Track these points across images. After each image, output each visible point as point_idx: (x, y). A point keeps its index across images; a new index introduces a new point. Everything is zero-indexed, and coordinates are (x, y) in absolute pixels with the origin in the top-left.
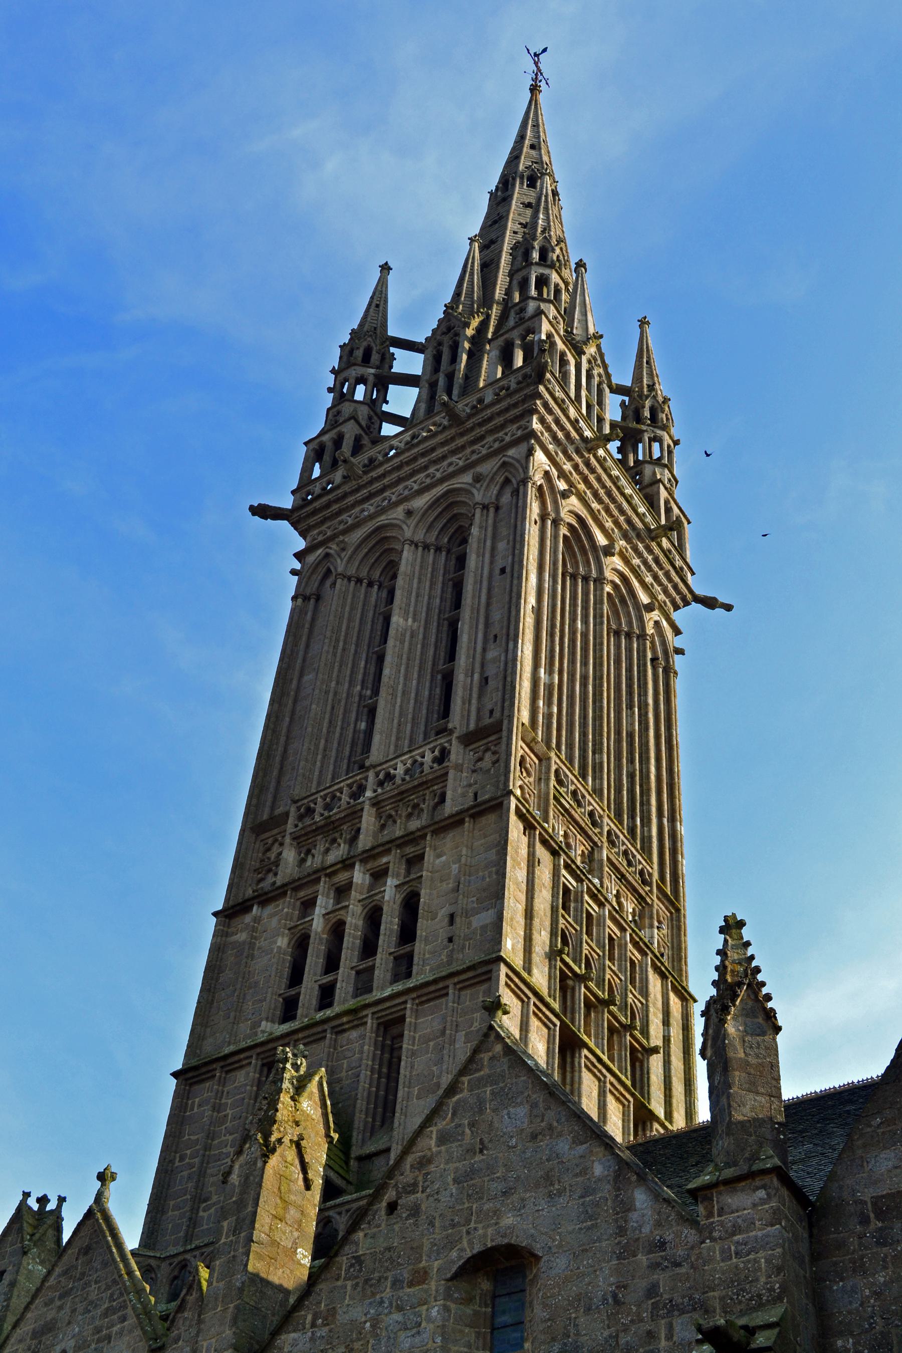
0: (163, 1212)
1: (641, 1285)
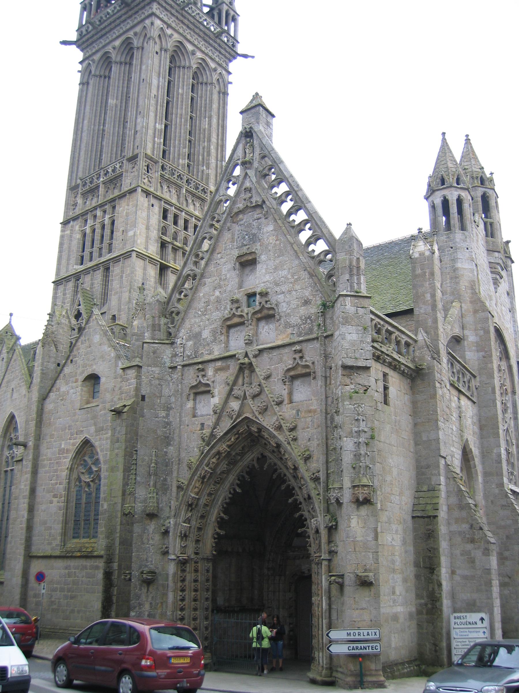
1: (118, 386)
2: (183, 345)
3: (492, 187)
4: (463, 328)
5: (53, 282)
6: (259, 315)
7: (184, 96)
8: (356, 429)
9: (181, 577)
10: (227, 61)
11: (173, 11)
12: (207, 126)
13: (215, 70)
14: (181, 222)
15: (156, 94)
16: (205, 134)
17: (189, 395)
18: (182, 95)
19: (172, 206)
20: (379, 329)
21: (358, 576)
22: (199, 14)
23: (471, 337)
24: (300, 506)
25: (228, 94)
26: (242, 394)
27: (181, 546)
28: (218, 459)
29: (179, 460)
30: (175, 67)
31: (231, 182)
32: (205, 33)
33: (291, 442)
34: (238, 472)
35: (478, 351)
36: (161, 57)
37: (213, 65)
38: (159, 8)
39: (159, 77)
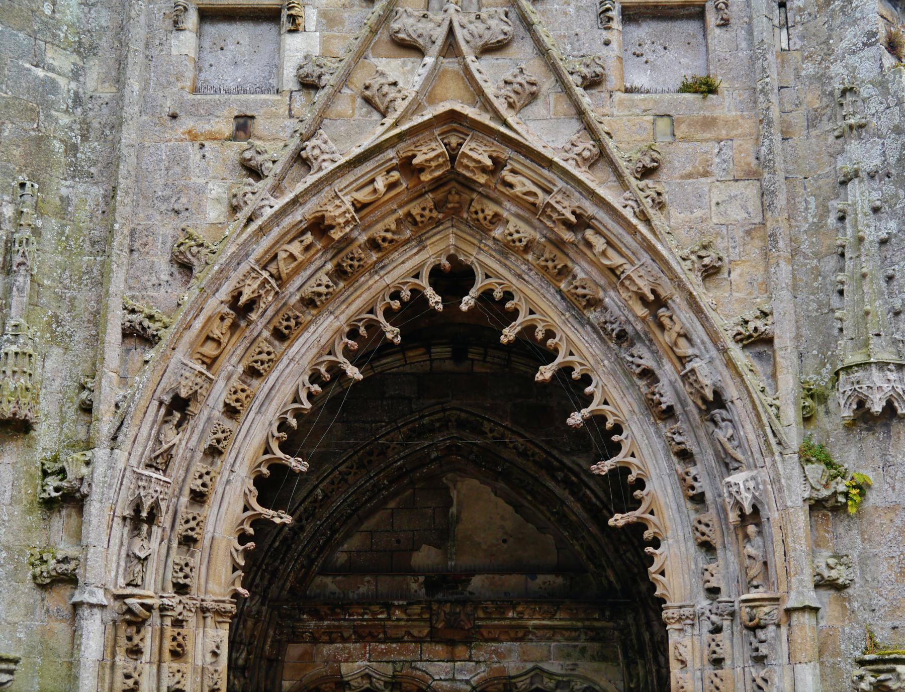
24: (615, 438)
26: (444, 29)
28: (307, 248)
33: (651, 212)
34: (354, 307)
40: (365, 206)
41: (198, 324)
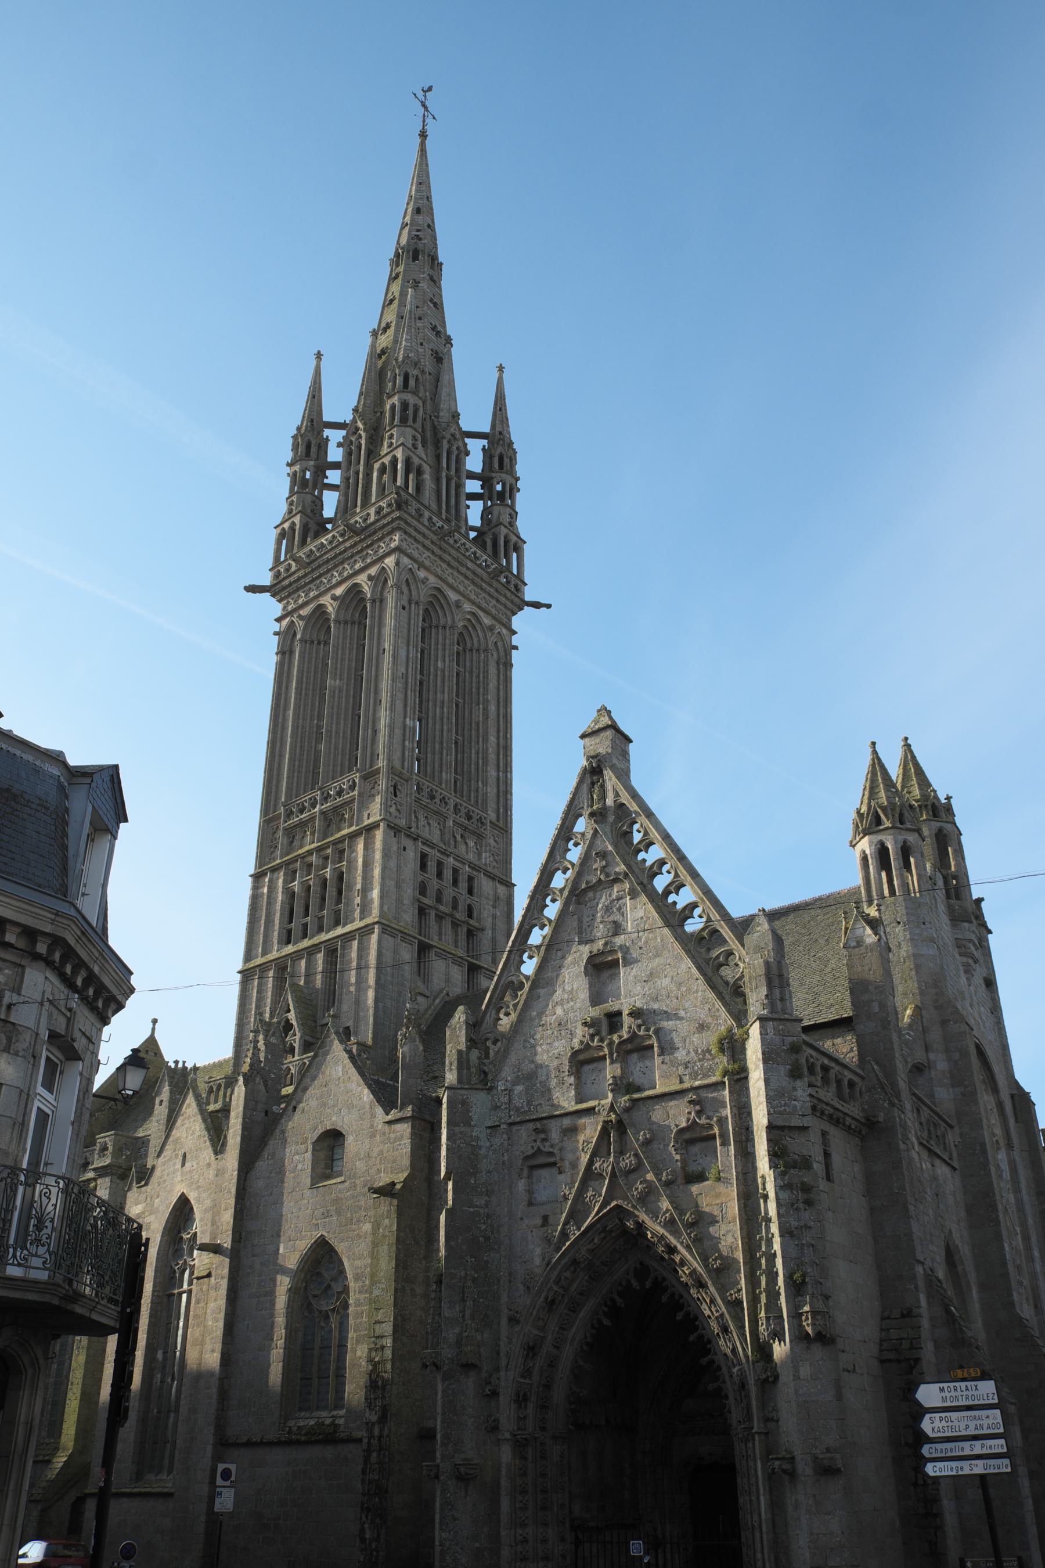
0: (241, 1046)
1: (376, 1150)
2: (509, 1092)
3: (952, 820)
4: (927, 1048)
5: (239, 972)
6: (629, 1046)
7: (447, 673)
8: (796, 1224)
9: (521, 1469)
10: (509, 613)
11: (427, 543)
12: (481, 719)
13: (491, 629)
14: (448, 874)
15: (404, 672)
16: (478, 731)
17: (522, 1169)
18: (443, 671)
19: (434, 848)
20: (813, 1064)
21: (816, 1458)
22: (464, 544)
23: (941, 1064)
24: (708, 1346)
25: (512, 665)
27: (518, 1417)
28: (574, 1271)
29: (510, 1274)
30: (430, 627)
31: (572, 842)
32: (474, 573)
35: (953, 1086)
36: (410, 614)
37: (487, 621)
38: (406, 540)
39: (408, 646)
40: (593, 1250)
41: (535, 1313)
